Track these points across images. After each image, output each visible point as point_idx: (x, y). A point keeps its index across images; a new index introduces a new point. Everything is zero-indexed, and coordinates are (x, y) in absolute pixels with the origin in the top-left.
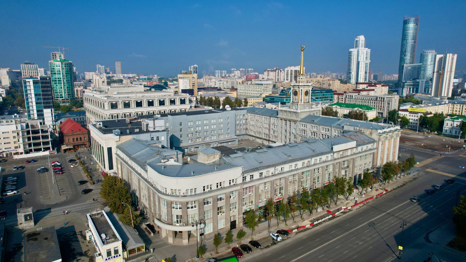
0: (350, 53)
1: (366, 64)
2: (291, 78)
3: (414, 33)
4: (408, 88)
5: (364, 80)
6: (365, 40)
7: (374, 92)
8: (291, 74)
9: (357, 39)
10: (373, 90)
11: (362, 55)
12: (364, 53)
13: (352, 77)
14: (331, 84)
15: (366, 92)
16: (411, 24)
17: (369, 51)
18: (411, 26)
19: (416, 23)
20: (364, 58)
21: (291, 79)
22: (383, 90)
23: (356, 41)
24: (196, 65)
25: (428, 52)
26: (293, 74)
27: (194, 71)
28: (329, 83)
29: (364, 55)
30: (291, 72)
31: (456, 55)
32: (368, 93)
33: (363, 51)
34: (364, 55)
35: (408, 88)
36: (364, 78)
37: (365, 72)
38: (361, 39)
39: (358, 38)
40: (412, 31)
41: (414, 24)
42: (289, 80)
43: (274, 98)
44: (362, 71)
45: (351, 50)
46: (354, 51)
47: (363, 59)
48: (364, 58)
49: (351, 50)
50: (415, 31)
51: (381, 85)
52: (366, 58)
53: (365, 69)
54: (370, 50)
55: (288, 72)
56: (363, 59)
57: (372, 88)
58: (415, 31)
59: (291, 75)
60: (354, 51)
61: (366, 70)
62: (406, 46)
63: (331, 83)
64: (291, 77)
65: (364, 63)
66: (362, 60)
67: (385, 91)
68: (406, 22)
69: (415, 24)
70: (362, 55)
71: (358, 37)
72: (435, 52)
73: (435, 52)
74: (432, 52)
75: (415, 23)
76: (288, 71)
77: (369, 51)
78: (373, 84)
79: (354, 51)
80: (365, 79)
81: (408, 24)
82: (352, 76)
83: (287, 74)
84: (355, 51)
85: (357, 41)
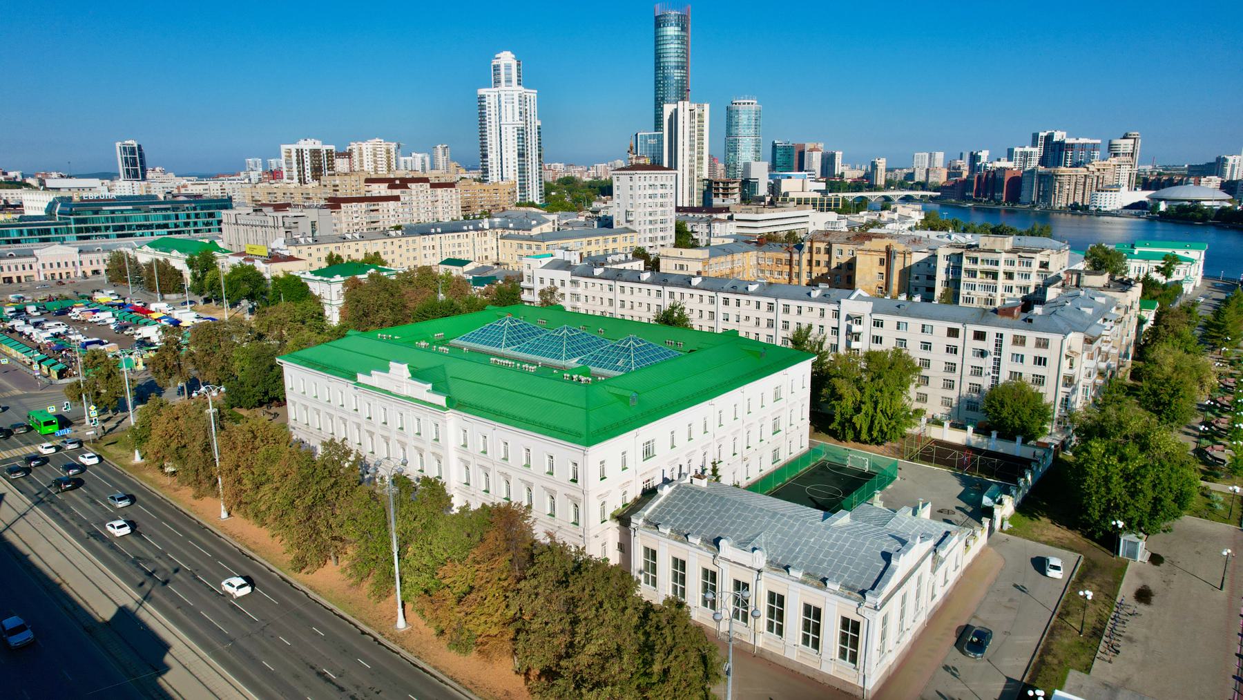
0: (482, 99)
1: (518, 130)
2: (299, 172)
3: (679, 51)
5: (517, 174)
6: (518, 65)
7: (400, 203)
8: (301, 161)
9: (495, 62)
10: (397, 198)
11: (509, 107)
13: (492, 167)
14: (337, 186)
15: (364, 205)
16: (669, 29)
17: (532, 94)
18: (671, 31)
19: (683, 24)
20: (513, 114)
21: (299, 175)
22: (440, 198)
23: (494, 66)
24: (130, 142)
25: (740, 104)
26: (294, 158)
27: (126, 159)
28: (333, 183)
29: (513, 106)
30: (298, 156)
31: (707, 107)
32: (372, 208)
33: (509, 95)
34: (513, 106)
36: (517, 168)
37: (517, 151)
38: (506, 59)
39: (497, 58)
40: (668, 46)
41: (676, 28)
42: (296, 180)
43: (8, 231)
45: (482, 92)
46: (489, 93)
48: (513, 114)
49: (482, 92)
50: (680, 46)
51: (428, 185)
52: (521, 113)
53: (516, 145)
54: (536, 91)
55: (290, 157)
57: (396, 192)
58: (680, 46)
59: (298, 164)
60: (489, 96)
61: (521, 147)
62: (664, 84)
63: (337, 182)
64: (301, 171)
66: (510, 120)
67: (446, 199)
68: (659, 22)
69: (680, 29)
70: (509, 107)
71: (497, 56)
72: (757, 104)
73: (757, 104)
74: (748, 103)
75: (678, 25)
76: (289, 152)
77: (532, 94)
78: (398, 182)
79: (489, 96)
80: (519, 172)
81: (664, 26)
82: (491, 163)
83: (288, 163)
84: (492, 95)
85: (497, 68)
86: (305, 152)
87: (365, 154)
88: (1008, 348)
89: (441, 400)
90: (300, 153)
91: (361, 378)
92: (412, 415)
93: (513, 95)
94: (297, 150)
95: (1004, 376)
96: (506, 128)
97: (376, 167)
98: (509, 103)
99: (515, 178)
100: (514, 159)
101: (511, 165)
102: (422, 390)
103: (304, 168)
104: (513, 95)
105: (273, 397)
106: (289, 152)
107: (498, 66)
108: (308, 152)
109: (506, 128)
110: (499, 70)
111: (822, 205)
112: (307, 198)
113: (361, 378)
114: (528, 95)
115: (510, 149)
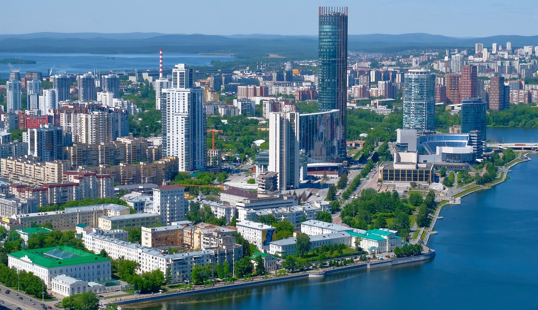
4: (262, 166)
12: (184, 97)
29: (184, 102)
30: (38, 137)
34: (184, 102)
35: (262, 166)
36: (184, 145)
44: (180, 132)
47: (184, 109)
56: (184, 109)
65: (182, 117)
66: (181, 111)
69: (336, 27)
71: (176, 66)
76: (32, 133)
79: (169, 93)
83: (32, 140)
84: (171, 92)
86: (43, 133)
87: (90, 122)
88: (160, 262)
89: (32, 262)
90: (40, 134)
91: (21, 258)
92: (28, 264)
93: (184, 94)
94: (38, 133)
95: (159, 267)
96: (177, 118)
97: (96, 133)
98: (181, 100)
99: (182, 152)
100: (182, 138)
101: (180, 143)
102: (29, 260)
103: (41, 144)
104: (184, 94)
105: (6, 263)
106: (32, 133)
107: (176, 73)
108: (45, 134)
109: (177, 118)
110: (176, 76)
111: (415, 176)
112: (38, 172)
113: (21, 258)
114: (197, 92)
115: (180, 132)
